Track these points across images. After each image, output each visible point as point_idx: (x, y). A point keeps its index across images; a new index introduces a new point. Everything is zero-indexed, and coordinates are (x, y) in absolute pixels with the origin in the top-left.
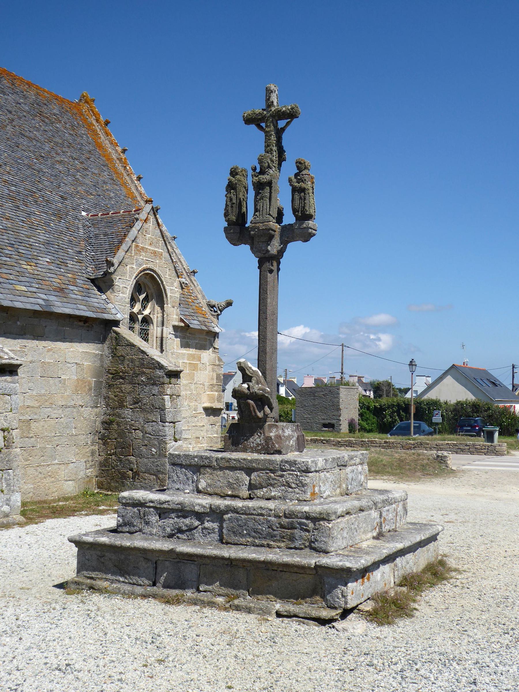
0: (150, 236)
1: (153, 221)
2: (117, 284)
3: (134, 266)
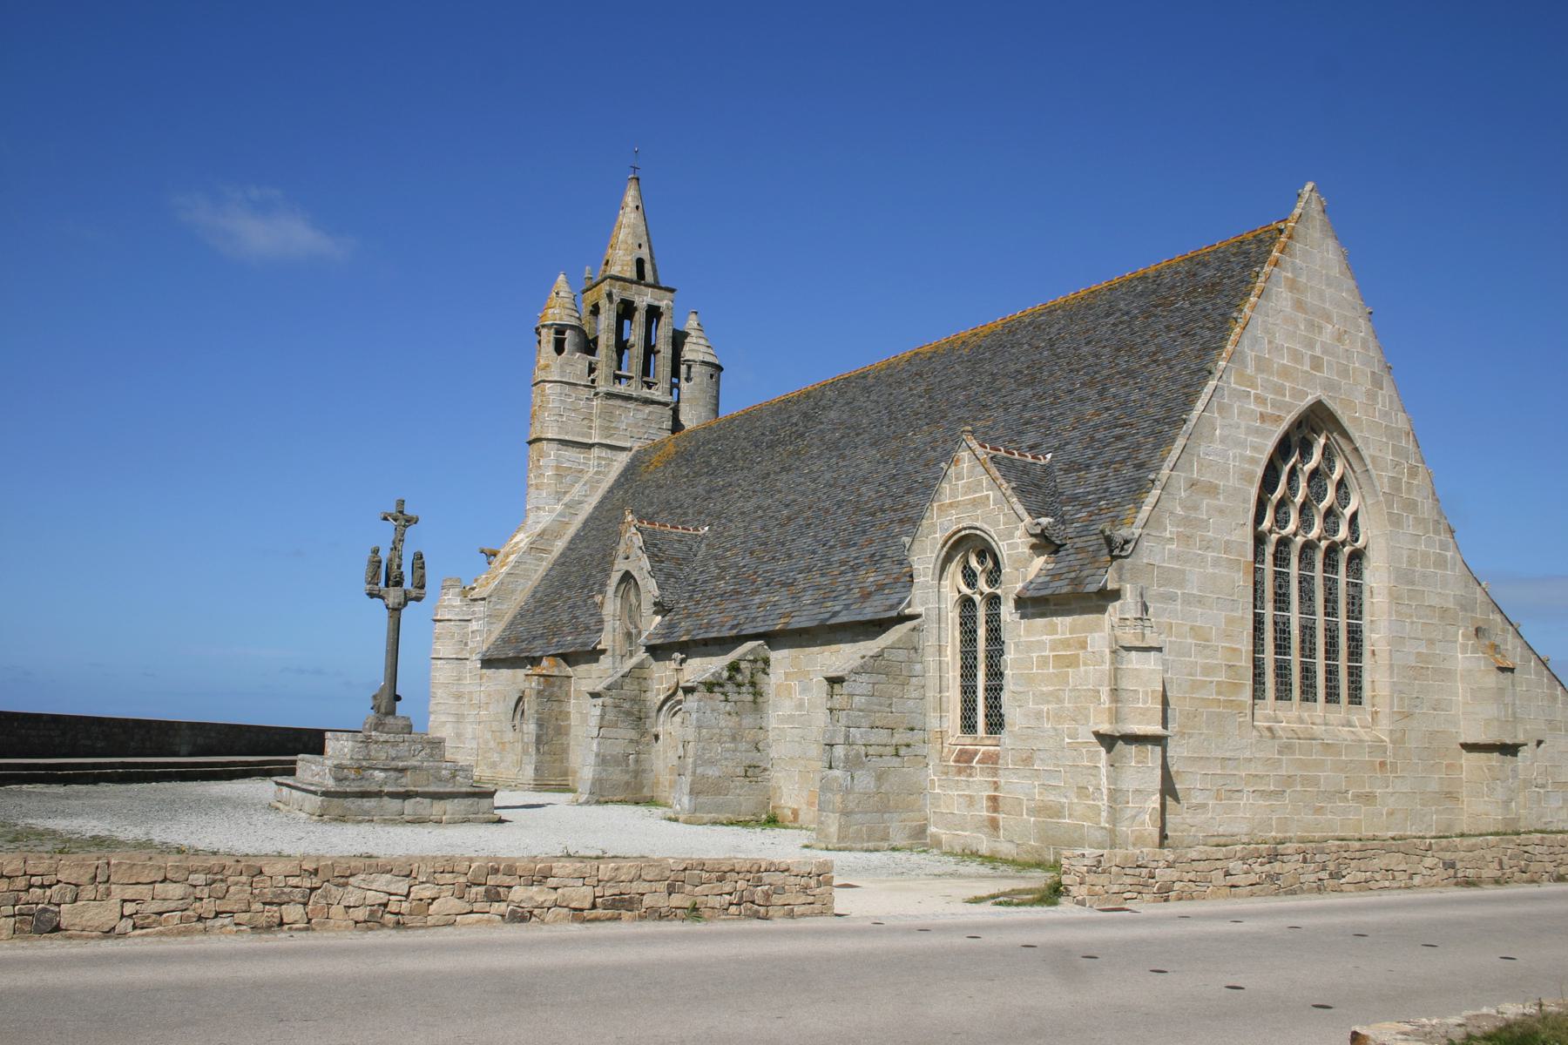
0: (965, 481)
1: (969, 459)
2: (916, 567)
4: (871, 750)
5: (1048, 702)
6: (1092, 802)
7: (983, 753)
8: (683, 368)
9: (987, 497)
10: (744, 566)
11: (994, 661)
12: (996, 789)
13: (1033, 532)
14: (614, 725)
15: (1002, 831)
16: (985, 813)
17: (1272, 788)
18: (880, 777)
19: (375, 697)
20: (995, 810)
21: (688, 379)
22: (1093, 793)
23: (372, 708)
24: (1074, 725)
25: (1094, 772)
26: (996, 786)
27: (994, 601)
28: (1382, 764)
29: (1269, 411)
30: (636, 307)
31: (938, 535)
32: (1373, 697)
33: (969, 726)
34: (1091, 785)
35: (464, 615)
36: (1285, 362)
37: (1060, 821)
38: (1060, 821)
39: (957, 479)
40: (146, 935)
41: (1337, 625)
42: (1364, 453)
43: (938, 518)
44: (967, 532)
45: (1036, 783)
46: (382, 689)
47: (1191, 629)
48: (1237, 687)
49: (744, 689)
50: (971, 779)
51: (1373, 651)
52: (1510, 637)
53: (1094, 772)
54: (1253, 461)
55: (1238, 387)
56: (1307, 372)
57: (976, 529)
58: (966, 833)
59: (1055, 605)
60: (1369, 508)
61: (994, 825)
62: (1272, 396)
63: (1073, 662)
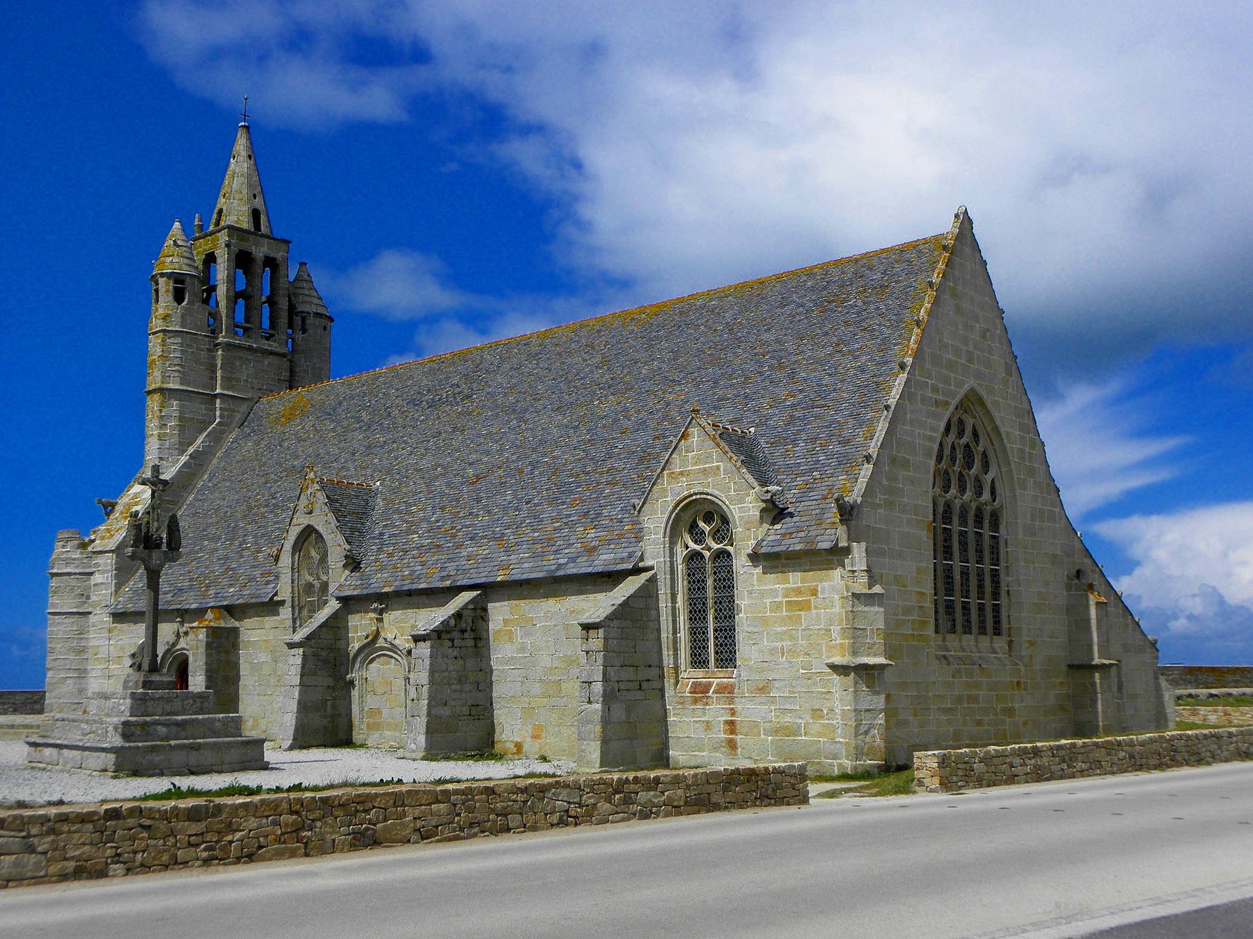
0: (695, 453)
1: (698, 434)
3: (669, 499)
4: (622, 686)
5: (782, 640)
6: (826, 722)
7: (717, 684)
8: (298, 320)
9: (718, 468)
10: (438, 521)
11: (723, 606)
12: (733, 714)
13: (764, 498)
14: (315, 674)
15: (739, 750)
16: (722, 736)
17: (950, 706)
18: (629, 710)
19: (133, 655)
20: (733, 732)
21: (304, 331)
22: (827, 714)
23: (131, 667)
24: (808, 659)
25: (827, 697)
26: (733, 712)
27: (722, 555)
28: (1018, 683)
29: (941, 398)
30: (253, 259)
31: (669, 499)
32: (1010, 628)
33: (698, 660)
34: (826, 707)
35: (84, 568)
36: (950, 356)
37: (796, 738)
38: (796, 738)
39: (687, 451)
40: (431, 842)
41: (983, 570)
42: (1002, 430)
43: (668, 485)
44: (698, 496)
45: (772, 708)
46: (142, 647)
47: (894, 577)
48: (923, 623)
49: (466, 635)
50: (708, 707)
51: (1008, 591)
52: (1097, 576)
53: (827, 697)
54: (931, 439)
55: (920, 378)
56: (962, 364)
57: (708, 494)
58: (703, 754)
59: (786, 560)
60: (1004, 474)
61: (732, 745)
62: (942, 385)
63: (805, 606)
